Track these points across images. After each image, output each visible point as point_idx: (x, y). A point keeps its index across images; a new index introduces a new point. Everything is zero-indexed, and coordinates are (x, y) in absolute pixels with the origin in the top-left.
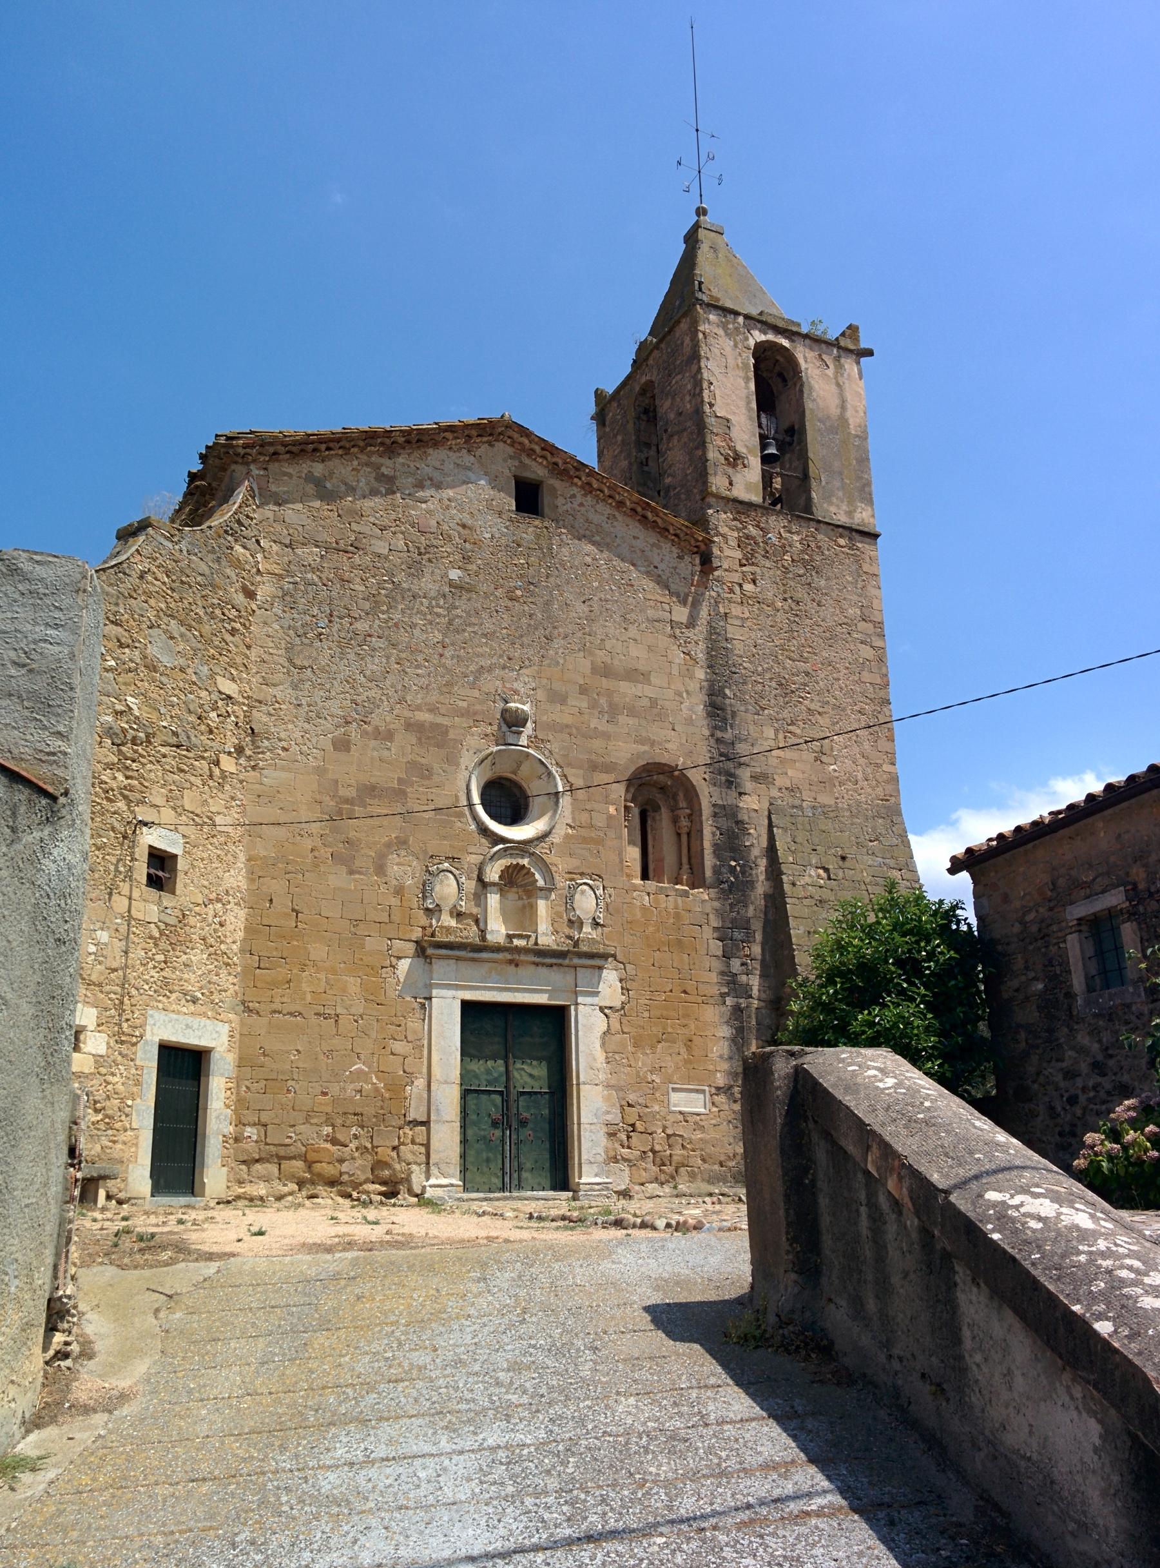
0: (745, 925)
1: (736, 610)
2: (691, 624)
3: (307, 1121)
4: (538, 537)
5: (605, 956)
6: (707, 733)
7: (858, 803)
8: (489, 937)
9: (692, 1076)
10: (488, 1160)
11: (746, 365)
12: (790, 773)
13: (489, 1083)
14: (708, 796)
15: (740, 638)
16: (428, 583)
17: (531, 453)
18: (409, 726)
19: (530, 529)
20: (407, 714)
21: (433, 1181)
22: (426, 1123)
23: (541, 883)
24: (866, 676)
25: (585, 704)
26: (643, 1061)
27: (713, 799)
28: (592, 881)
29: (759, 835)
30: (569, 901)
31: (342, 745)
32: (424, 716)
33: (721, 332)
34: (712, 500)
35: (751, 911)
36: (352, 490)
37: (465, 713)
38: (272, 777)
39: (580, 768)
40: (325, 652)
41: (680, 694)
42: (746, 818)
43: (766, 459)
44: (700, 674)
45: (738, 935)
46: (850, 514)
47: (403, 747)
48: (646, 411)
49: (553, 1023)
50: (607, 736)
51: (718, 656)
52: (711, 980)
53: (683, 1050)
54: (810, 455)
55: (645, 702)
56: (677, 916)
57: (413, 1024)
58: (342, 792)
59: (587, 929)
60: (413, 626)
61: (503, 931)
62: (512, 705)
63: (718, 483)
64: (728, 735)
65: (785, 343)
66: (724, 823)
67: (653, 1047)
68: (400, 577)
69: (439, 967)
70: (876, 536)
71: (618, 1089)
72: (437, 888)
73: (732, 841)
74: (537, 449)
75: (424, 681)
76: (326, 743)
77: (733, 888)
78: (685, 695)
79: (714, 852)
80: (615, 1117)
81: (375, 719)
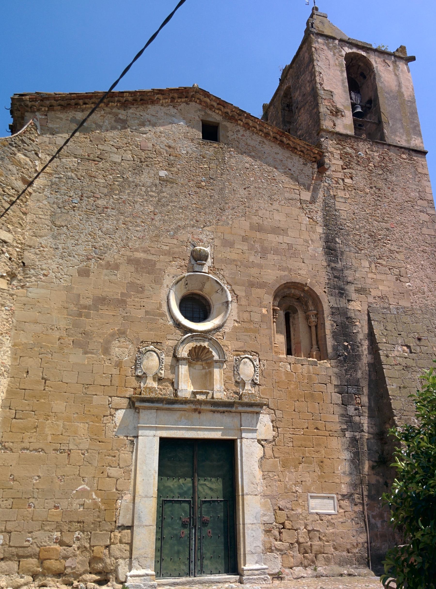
0: (356, 384)
1: (341, 193)
2: (313, 201)
3: (42, 528)
4: (216, 153)
5: (260, 405)
6: (325, 264)
7: (426, 306)
8: (179, 394)
9: (324, 487)
10: (178, 552)
11: (340, 65)
12: (380, 288)
13: (181, 495)
14: (327, 302)
15: (344, 208)
16: (146, 178)
17: (211, 107)
18: (130, 261)
19: (210, 149)
20: (129, 253)
21: (134, 572)
22: (130, 528)
23: (216, 357)
24: (425, 230)
25: (246, 248)
26: (289, 477)
27: (331, 304)
28: (251, 355)
29: (362, 326)
30: (236, 368)
31: (84, 273)
32: (140, 255)
33: (325, 47)
34: (323, 133)
35: (359, 374)
36: (99, 127)
37: (168, 253)
38: (34, 292)
39: (243, 285)
40: (76, 218)
41: (307, 242)
42: (353, 315)
43: (355, 115)
44: (320, 230)
45: (351, 390)
46: (408, 141)
47: (125, 274)
48: (288, 106)
49: (227, 450)
50: (260, 266)
51: (330, 220)
52: (335, 420)
53: (317, 469)
54: (382, 110)
55: (285, 246)
57: (125, 455)
58: (82, 302)
59: (248, 387)
60: (135, 202)
61: (191, 389)
62: (198, 248)
63: (326, 124)
64: (339, 265)
65: (364, 54)
66: (339, 319)
67: (295, 467)
68: (128, 175)
69: (144, 414)
70: (424, 153)
71: (272, 497)
72: (145, 362)
73: (344, 329)
74: (215, 104)
75: (141, 234)
76: (74, 271)
77: (346, 359)
78: (310, 242)
79: (333, 337)
80: (269, 518)
81: (108, 257)
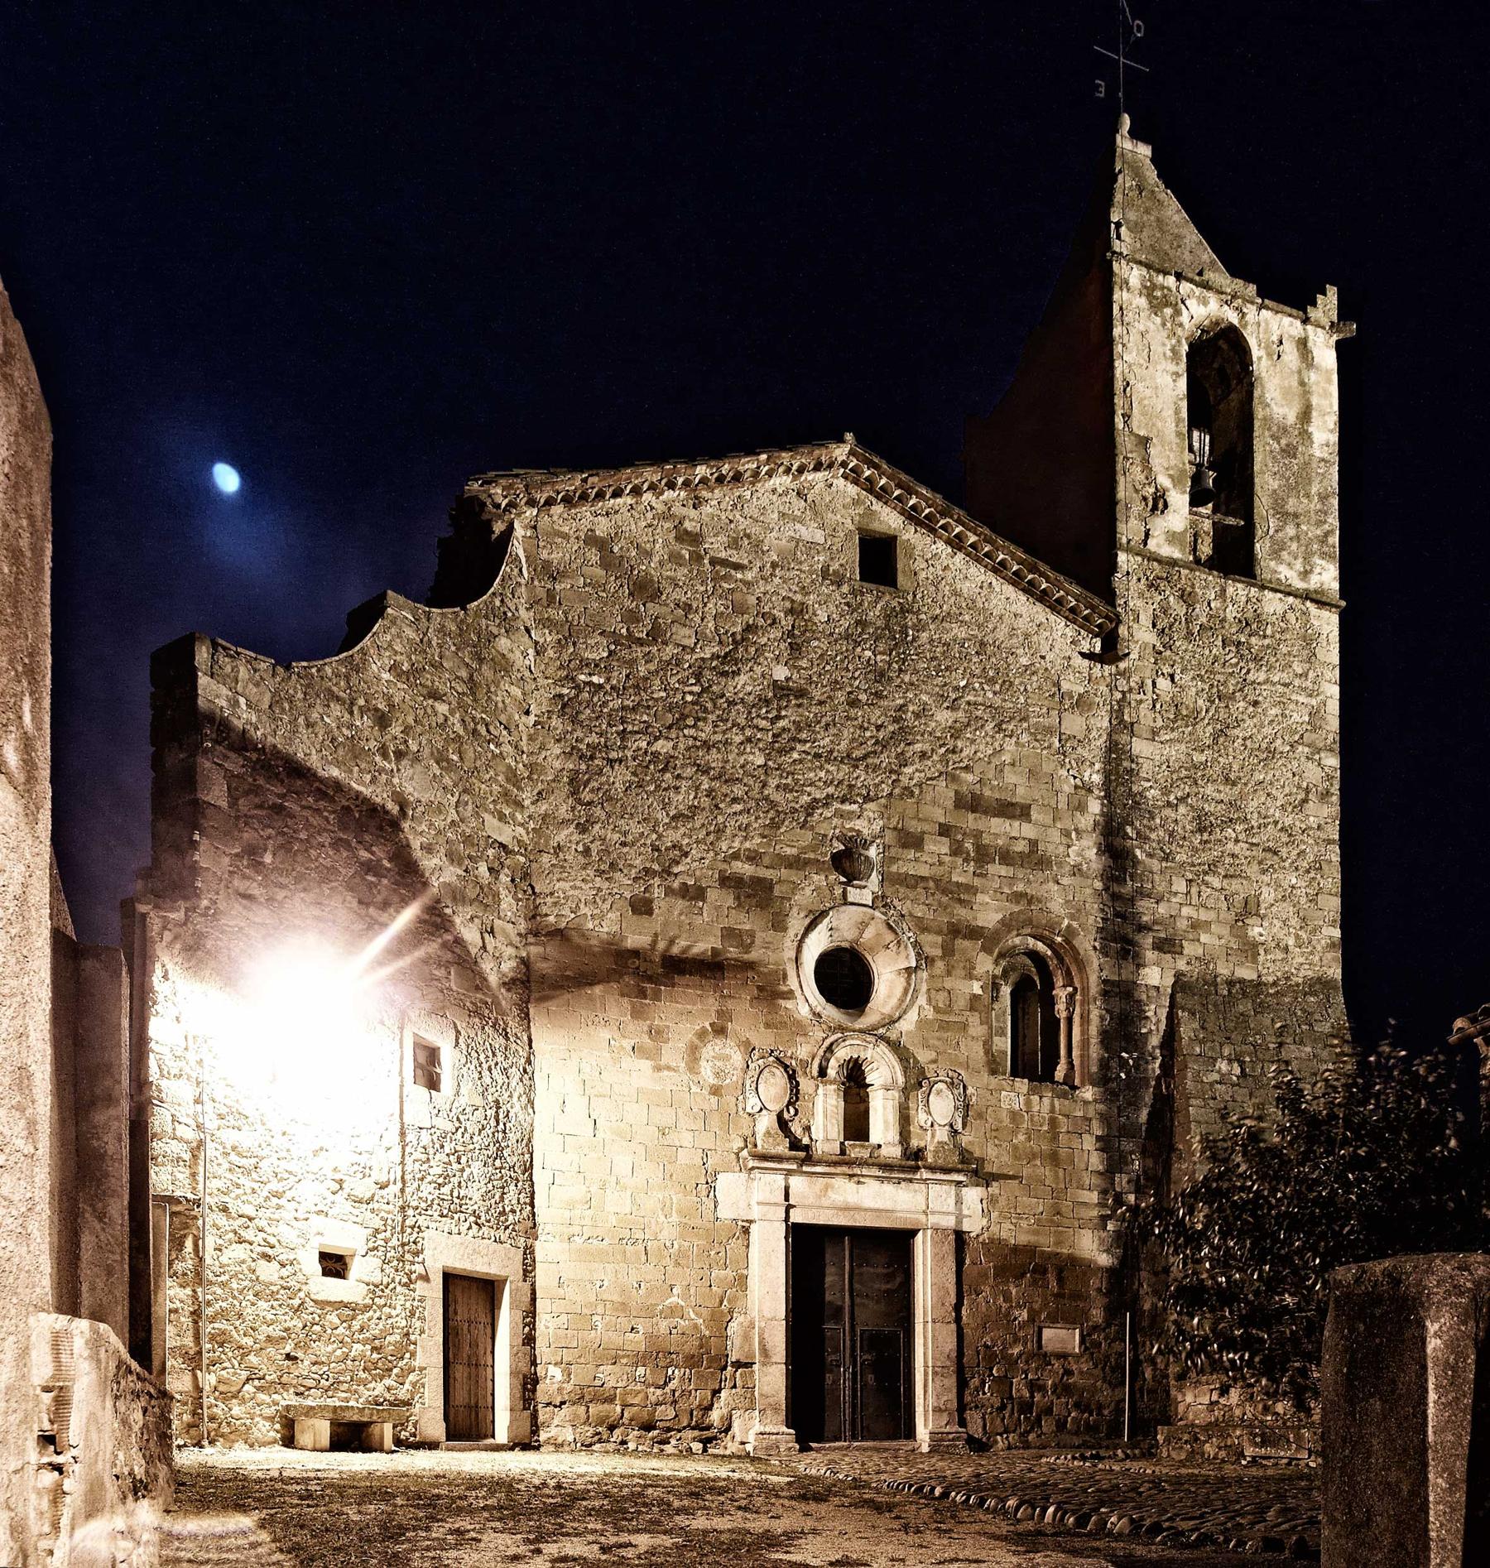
12: (1203, 939)
25: (945, 850)
27: (1104, 975)
29: (1159, 1021)
39: (939, 933)
41: (1068, 835)
42: (1144, 997)
44: (1095, 807)
56: (1053, 1122)
64: (1128, 887)
78: (1074, 835)
79: (1102, 1042)
